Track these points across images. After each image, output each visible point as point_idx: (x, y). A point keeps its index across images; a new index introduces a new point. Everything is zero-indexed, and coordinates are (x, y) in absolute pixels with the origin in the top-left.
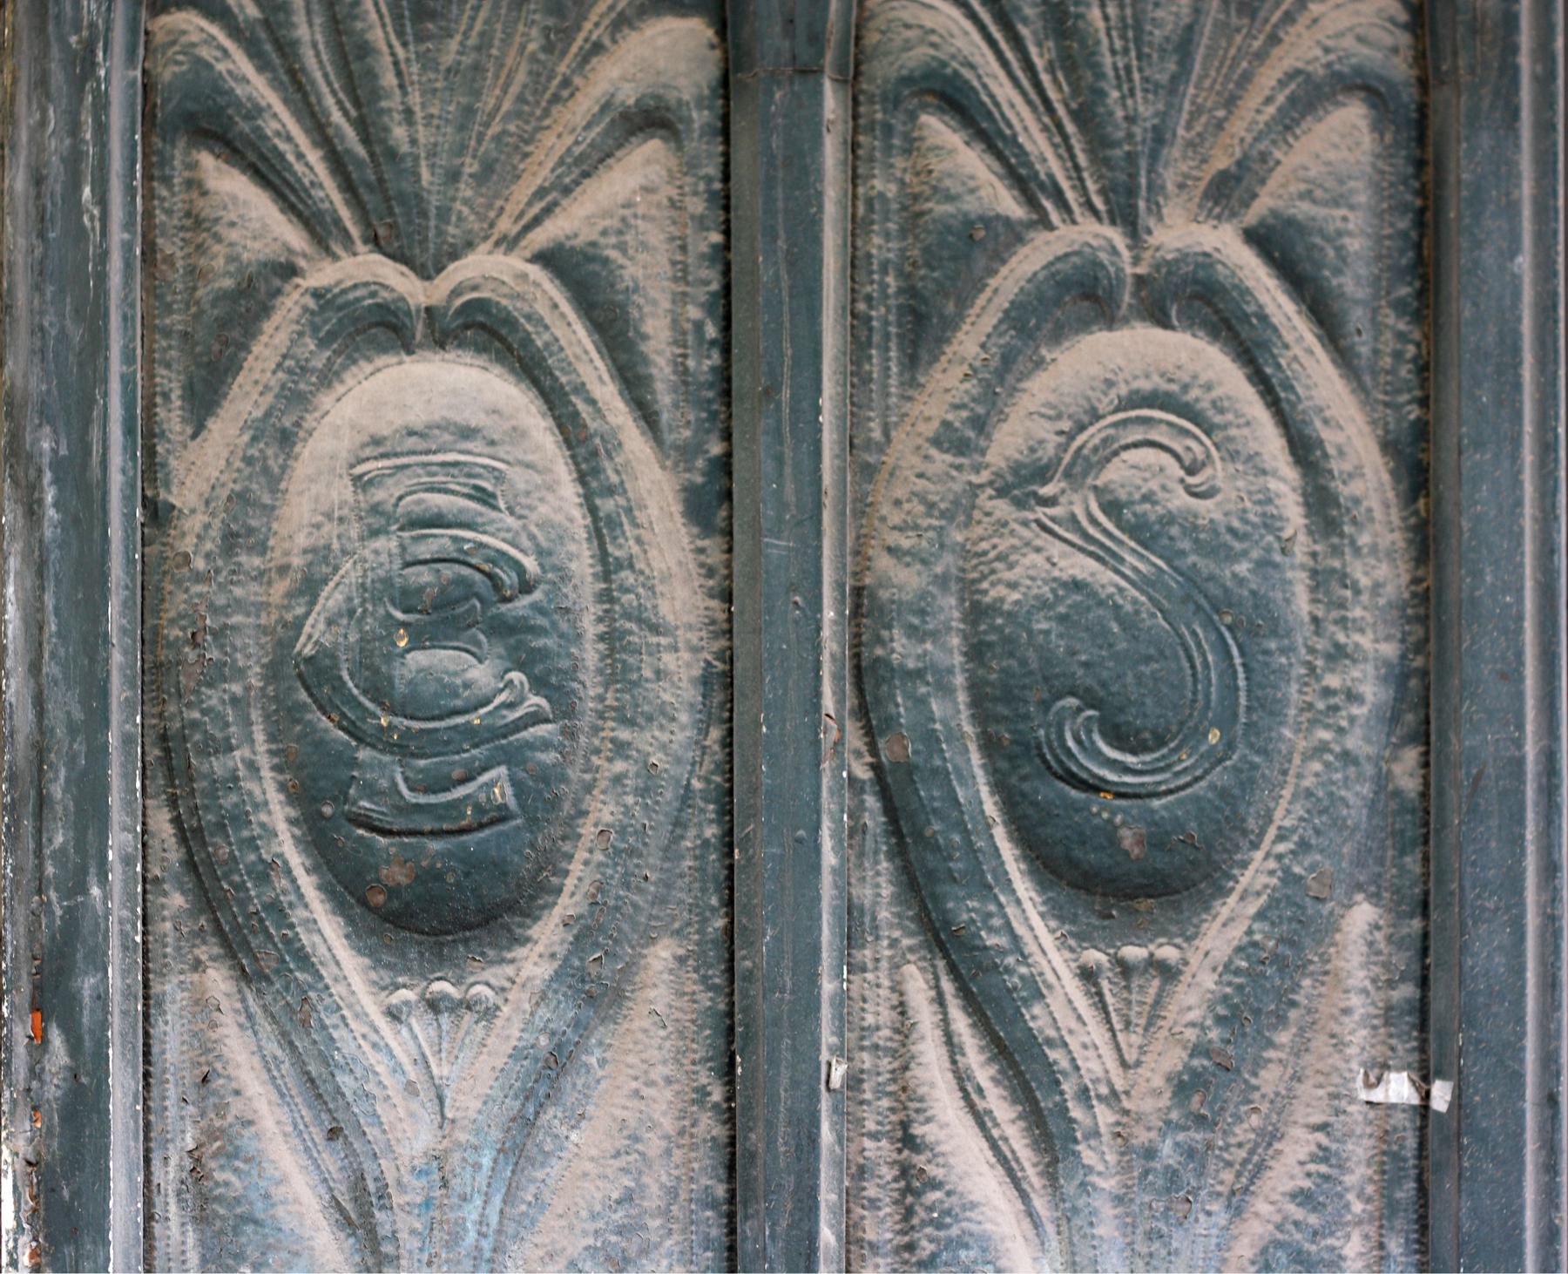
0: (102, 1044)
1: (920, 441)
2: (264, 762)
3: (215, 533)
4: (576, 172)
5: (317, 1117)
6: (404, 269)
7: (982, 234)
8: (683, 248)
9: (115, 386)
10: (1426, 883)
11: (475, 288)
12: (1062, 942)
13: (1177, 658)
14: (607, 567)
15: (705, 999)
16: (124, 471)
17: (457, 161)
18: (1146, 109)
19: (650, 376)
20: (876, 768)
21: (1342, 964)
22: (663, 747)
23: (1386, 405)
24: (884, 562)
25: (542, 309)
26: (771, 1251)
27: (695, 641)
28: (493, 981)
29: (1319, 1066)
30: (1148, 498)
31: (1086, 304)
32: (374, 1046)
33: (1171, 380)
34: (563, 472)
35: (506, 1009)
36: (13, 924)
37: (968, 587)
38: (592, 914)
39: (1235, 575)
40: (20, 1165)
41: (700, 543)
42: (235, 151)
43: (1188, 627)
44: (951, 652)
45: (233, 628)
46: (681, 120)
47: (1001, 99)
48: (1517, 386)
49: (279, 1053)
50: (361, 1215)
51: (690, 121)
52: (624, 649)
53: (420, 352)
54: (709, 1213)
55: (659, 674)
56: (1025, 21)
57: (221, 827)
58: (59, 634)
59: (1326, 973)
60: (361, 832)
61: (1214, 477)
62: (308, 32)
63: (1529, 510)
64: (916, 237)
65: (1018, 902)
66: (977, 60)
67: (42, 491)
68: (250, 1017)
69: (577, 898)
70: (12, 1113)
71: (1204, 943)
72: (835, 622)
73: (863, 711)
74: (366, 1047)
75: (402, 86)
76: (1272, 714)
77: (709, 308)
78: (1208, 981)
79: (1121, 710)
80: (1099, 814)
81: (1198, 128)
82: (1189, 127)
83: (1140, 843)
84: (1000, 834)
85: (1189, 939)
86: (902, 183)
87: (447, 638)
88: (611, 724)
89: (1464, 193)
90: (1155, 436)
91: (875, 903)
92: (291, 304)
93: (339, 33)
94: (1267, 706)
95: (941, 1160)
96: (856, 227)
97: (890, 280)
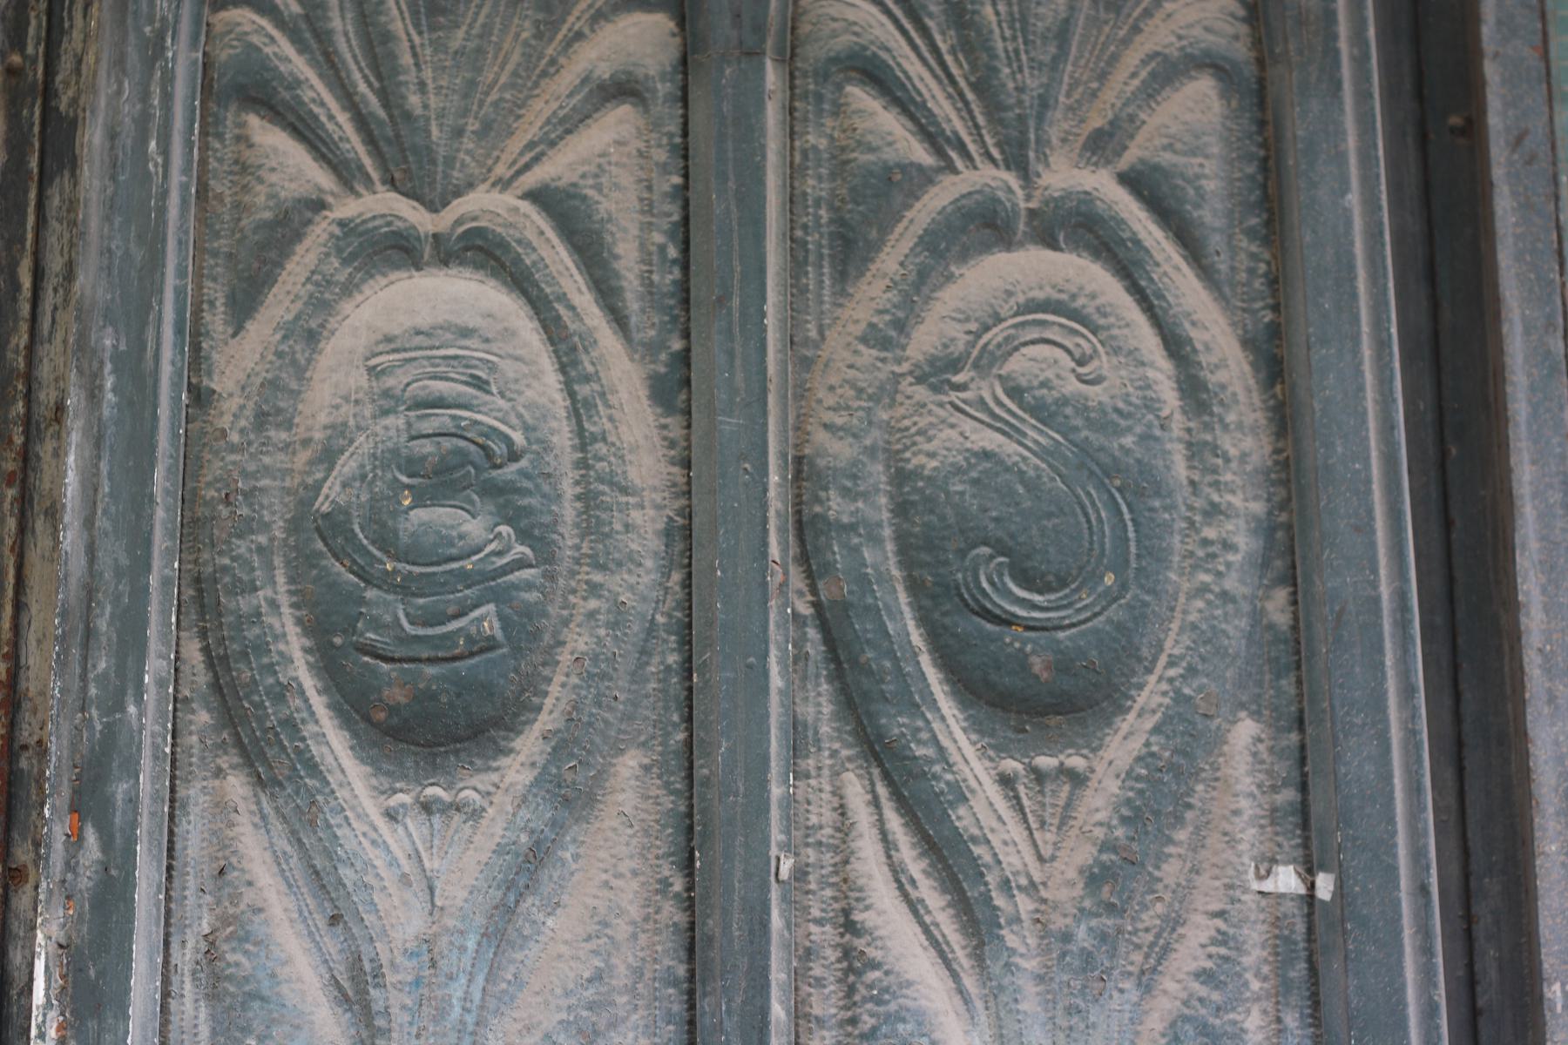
0: (131, 841)
1: (850, 339)
2: (284, 600)
3: (249, 412)
4: (560, 130)
5: (321, 905)
6: (416, 204)
7: (899, 177)
8: (649, 188)
9: (169, 295)
10: (1300, 702)
11: (474, 219)
12: (982, 753)
13: (1075, 515)
14: (584, 441)
15: (668, 802)
16: (173, 363)
17: (462, 122)
18: (1033, 82)
19: (621, 289)
20: (817, 605)
21: (1230, 771)
22: (631, 588)
23: (1244, 310)
24: (821, 436)
25: (530, 235)
26: (727, 1025)
27: (659, 500)
28: (480, 786)
29: (1214, 860)
30: (1044, 384)
31: (988, 231)
32: (373, 842)
33: (1061, 291)
34: (547, 364)
35: (491, 811)
36: (58, 738)
37: (893, 457)
38: (567, 729)
39: (1121, 447)
40: (52, 947)
41: (663, 421)
42: (278, 113)
43: (1083, 489)
44: (879, 509)
45: (261, 490)
46: (648, 90)
47: (912, 74)
48: (1354, 296)
49: (288, 849)
50: (357, 992)
51: (654, 91)
52: (598, 507)
53: (428, 270)
54: (671, 991)
55: (627, 527)
56: (931, 16)
57: (244, 655)
58: (111, 495)
59: (1217, 779)
60: (366, 659)
61: (1101, 368)
62: (341, 24)
63: (1370, 394)
64: (844, 180)
65: (943, 719)
66: (892, 44)
67: (103, 379)
68: (264, 817)
69: (555, 715)
70: (48, 901)
71: (1108, 754)
72: (779, 485)
73: (804, 558)
74: (366, 843)
75: (417, 65)
76: (1159, 560)
77: (671, 235)
78: (1113, 786)
79: (1028, 557)
80: (1011, 644)
81: (1076, 96)
82: (1068, 95)
83: (1048, 668)
84: (925, 661)
85: (1094, 750)
86: (832, 138)
87: (445, 497)
88: (586, 569)
89: (1300, 146)
90: (1048, 335)
91: (817, 720)
92: (320, 231)
93: (366, 25)
94: (1155, 554)
95: (879, 943)
96: (794, 172)
97: (823, 212)
